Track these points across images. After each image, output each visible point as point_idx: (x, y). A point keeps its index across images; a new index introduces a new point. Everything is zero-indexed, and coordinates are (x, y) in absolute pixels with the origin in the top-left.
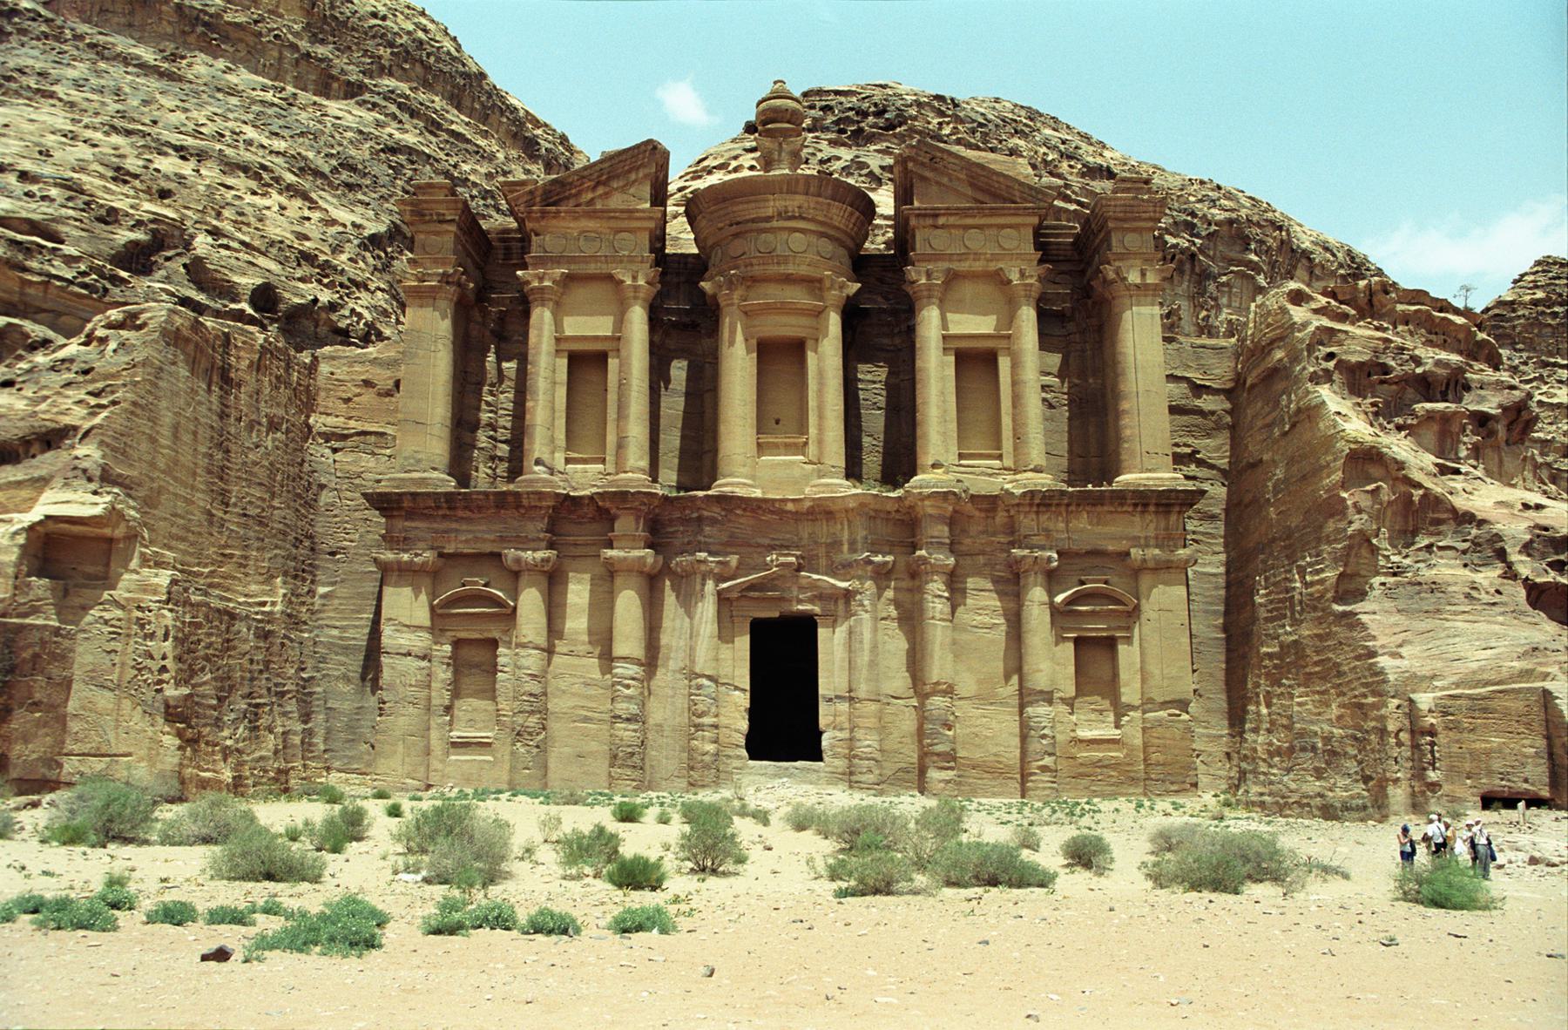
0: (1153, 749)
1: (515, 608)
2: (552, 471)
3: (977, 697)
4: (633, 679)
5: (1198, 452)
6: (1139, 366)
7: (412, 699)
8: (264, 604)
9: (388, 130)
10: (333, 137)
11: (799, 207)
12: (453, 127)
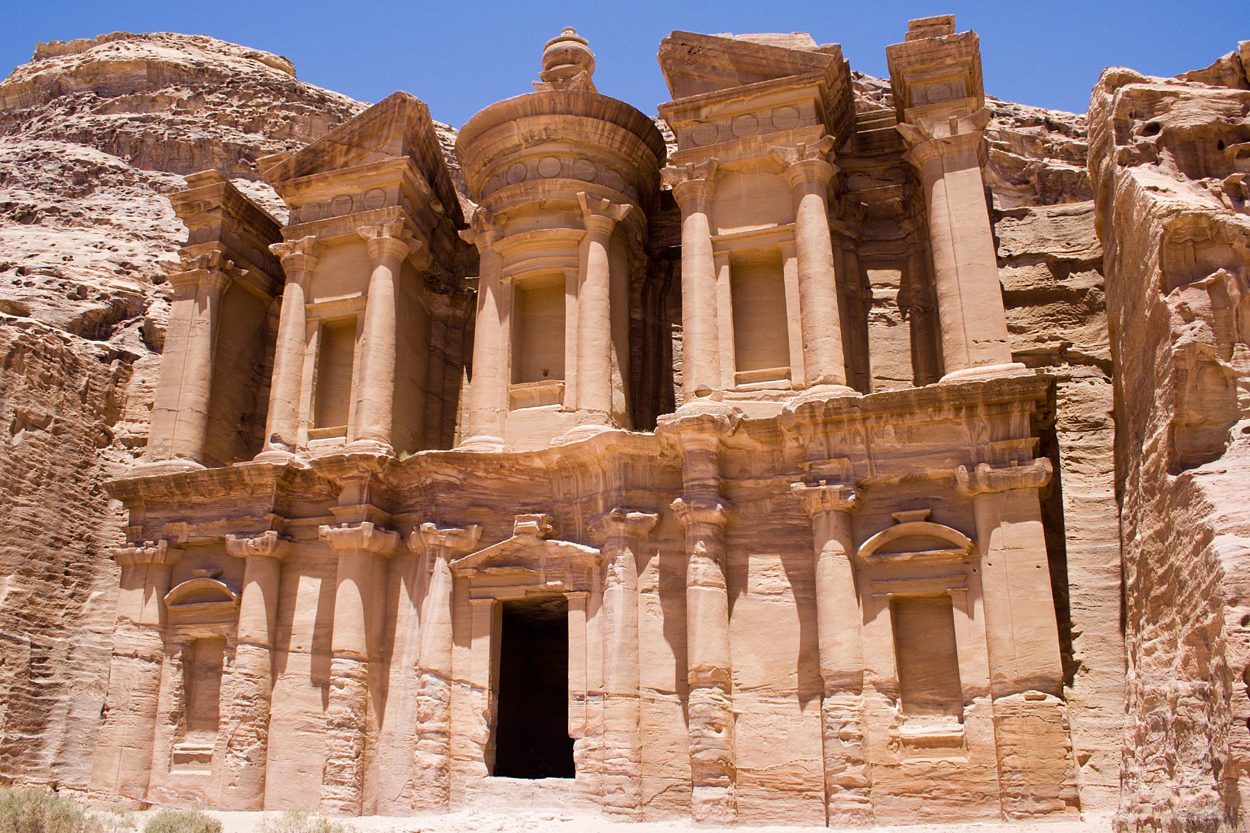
0: (1007, 750)
2: (292, 448)
3: (765, 687)
4: (348, 676)
5: (1070, 345)
7: (131, 705)
11: (545, 129)
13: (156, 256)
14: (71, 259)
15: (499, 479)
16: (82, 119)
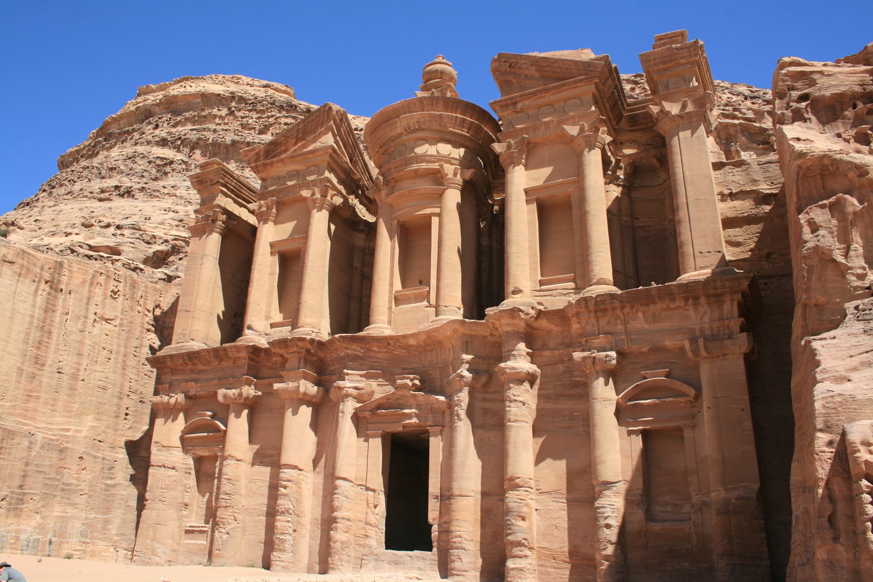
1: (225, 432)
6: (688, 180)
11: (418, 122)
14: (149, 219)
15: (388, 352)
16: (162, 133)
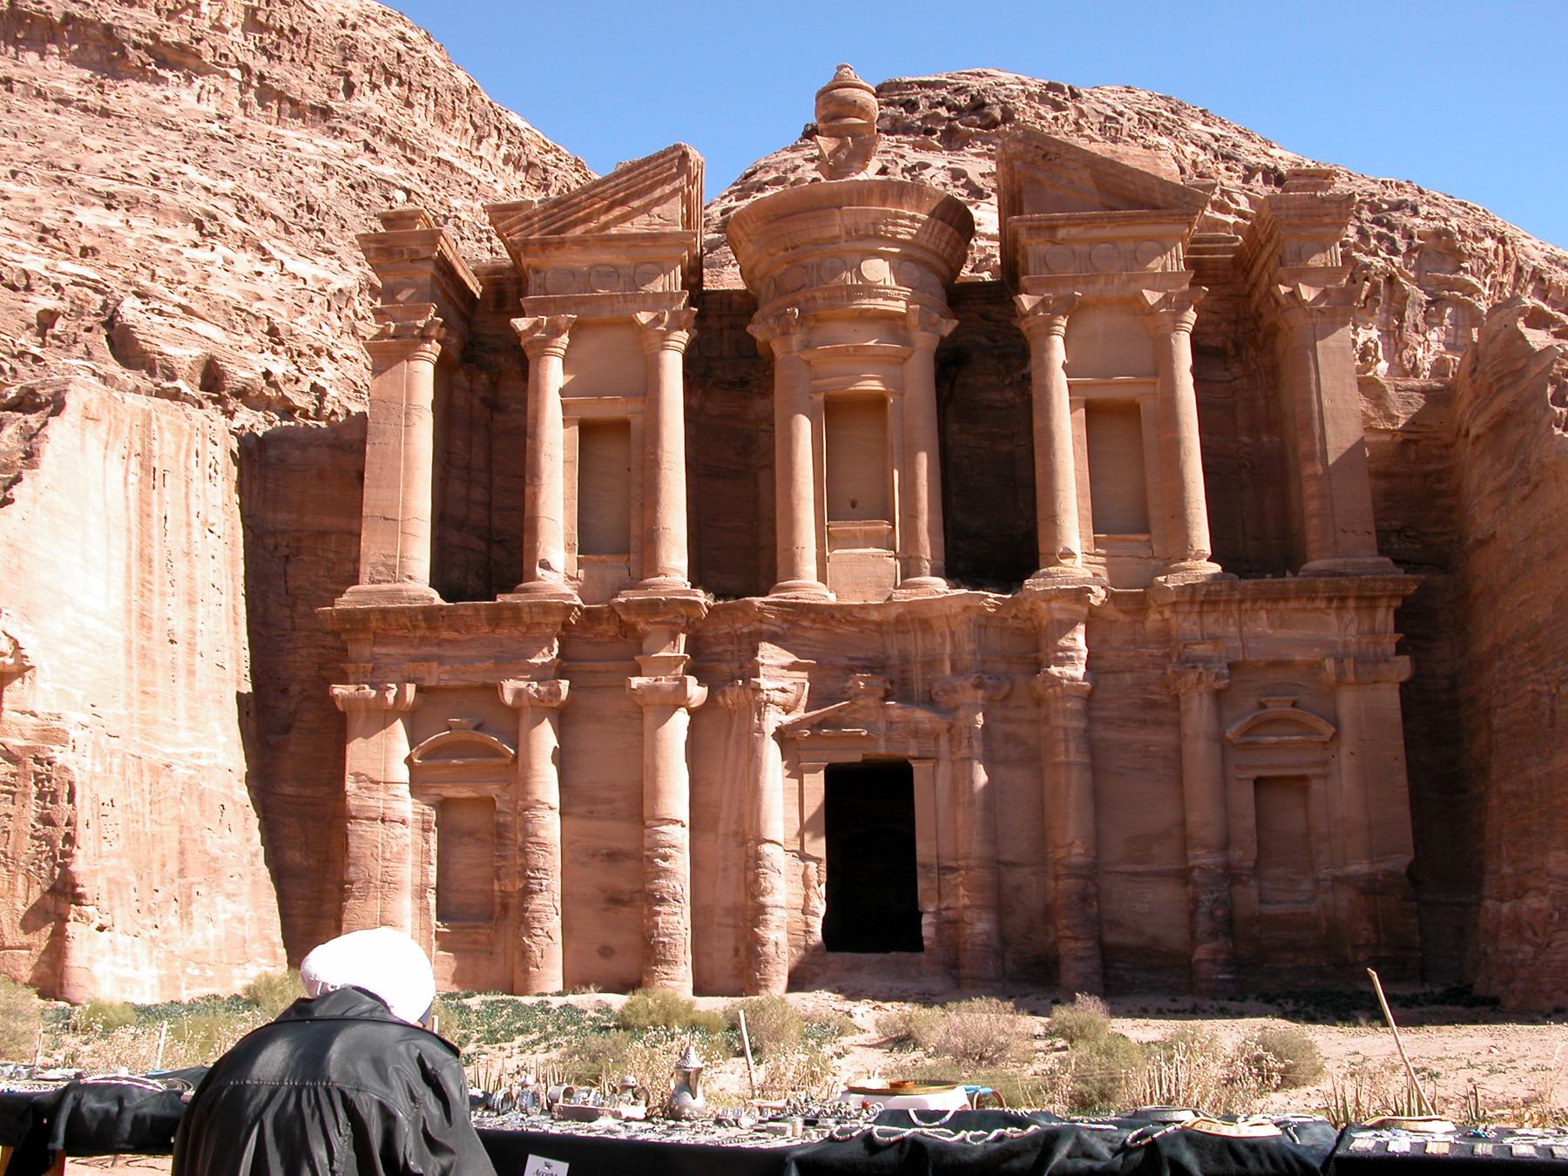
1: (516, 757)
6: (1327, 414)
8: (198, 756)
9: (359, 161)
10: (290, 173)
12: (441, 154)
13: (70, 212)
